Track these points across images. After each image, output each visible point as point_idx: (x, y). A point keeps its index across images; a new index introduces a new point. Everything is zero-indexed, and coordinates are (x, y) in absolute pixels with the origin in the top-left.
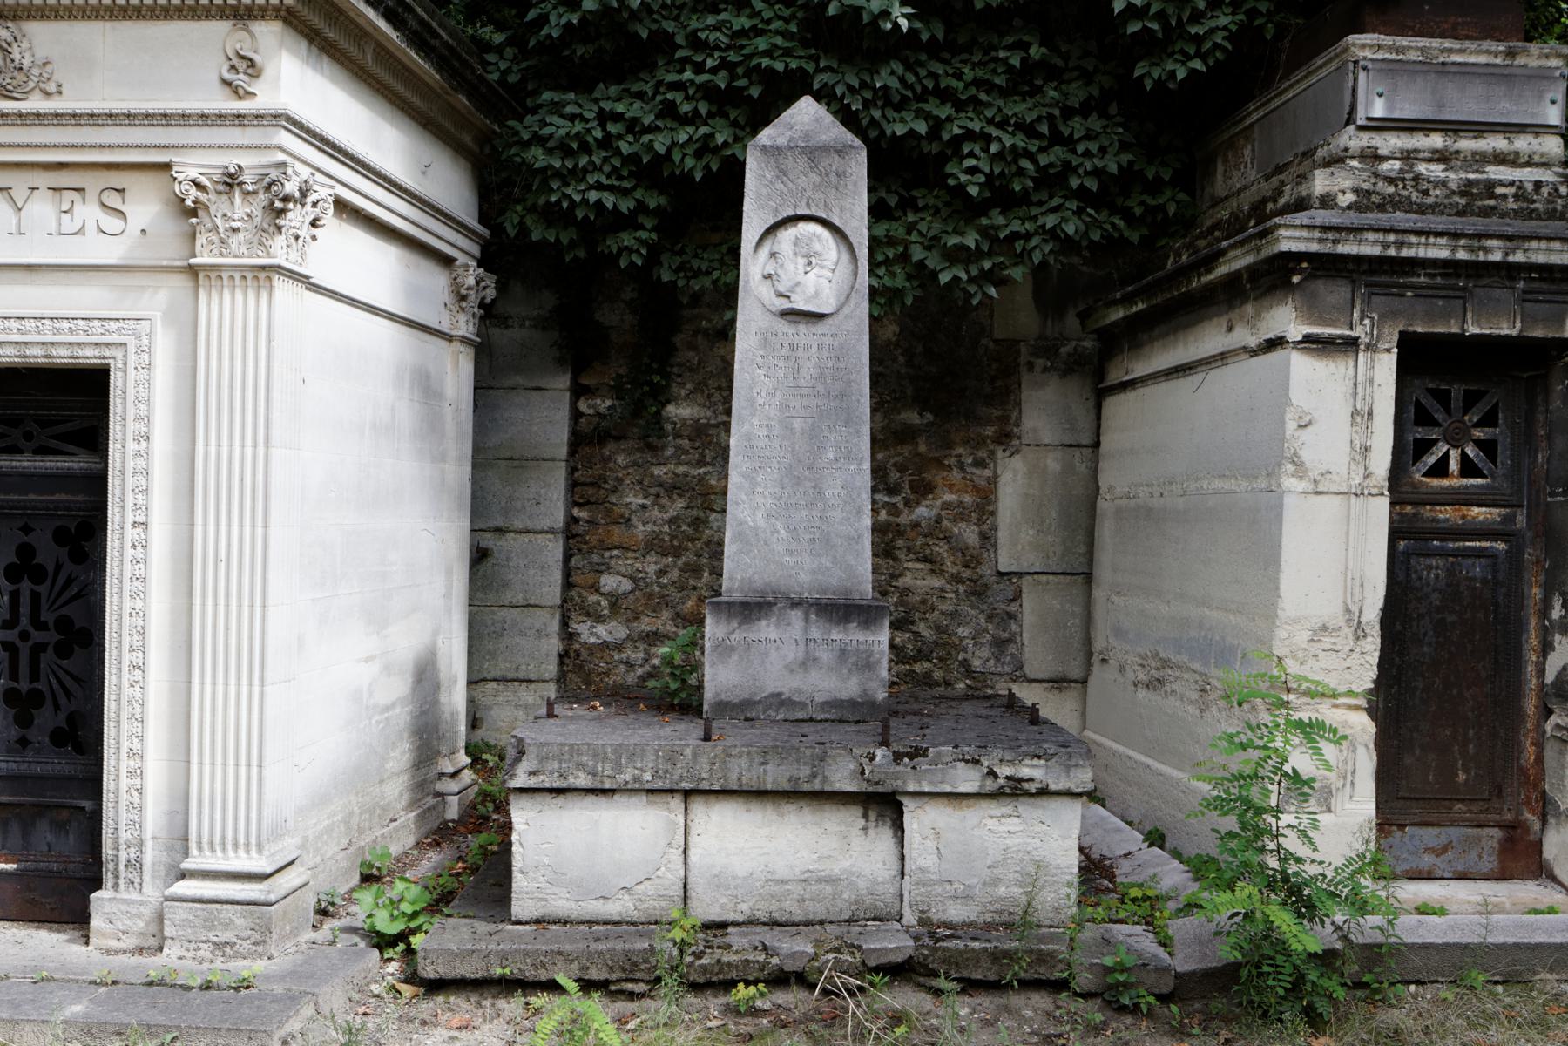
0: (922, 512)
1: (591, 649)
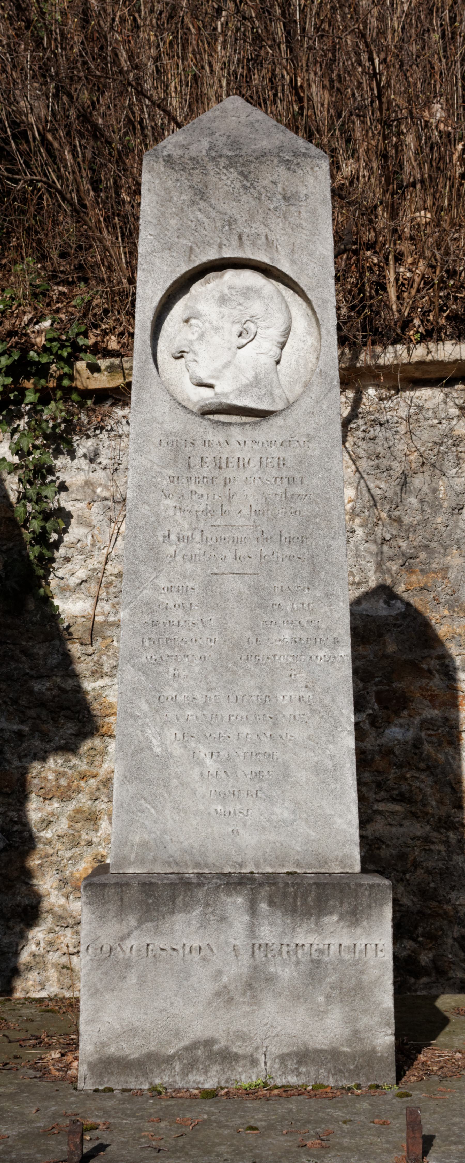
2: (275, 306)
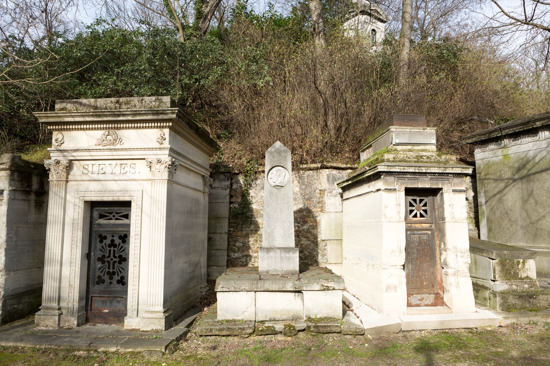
0: (305, 227)
1: (234, 259)
2: (284, 172)
